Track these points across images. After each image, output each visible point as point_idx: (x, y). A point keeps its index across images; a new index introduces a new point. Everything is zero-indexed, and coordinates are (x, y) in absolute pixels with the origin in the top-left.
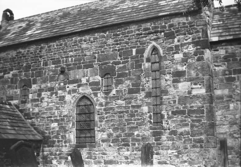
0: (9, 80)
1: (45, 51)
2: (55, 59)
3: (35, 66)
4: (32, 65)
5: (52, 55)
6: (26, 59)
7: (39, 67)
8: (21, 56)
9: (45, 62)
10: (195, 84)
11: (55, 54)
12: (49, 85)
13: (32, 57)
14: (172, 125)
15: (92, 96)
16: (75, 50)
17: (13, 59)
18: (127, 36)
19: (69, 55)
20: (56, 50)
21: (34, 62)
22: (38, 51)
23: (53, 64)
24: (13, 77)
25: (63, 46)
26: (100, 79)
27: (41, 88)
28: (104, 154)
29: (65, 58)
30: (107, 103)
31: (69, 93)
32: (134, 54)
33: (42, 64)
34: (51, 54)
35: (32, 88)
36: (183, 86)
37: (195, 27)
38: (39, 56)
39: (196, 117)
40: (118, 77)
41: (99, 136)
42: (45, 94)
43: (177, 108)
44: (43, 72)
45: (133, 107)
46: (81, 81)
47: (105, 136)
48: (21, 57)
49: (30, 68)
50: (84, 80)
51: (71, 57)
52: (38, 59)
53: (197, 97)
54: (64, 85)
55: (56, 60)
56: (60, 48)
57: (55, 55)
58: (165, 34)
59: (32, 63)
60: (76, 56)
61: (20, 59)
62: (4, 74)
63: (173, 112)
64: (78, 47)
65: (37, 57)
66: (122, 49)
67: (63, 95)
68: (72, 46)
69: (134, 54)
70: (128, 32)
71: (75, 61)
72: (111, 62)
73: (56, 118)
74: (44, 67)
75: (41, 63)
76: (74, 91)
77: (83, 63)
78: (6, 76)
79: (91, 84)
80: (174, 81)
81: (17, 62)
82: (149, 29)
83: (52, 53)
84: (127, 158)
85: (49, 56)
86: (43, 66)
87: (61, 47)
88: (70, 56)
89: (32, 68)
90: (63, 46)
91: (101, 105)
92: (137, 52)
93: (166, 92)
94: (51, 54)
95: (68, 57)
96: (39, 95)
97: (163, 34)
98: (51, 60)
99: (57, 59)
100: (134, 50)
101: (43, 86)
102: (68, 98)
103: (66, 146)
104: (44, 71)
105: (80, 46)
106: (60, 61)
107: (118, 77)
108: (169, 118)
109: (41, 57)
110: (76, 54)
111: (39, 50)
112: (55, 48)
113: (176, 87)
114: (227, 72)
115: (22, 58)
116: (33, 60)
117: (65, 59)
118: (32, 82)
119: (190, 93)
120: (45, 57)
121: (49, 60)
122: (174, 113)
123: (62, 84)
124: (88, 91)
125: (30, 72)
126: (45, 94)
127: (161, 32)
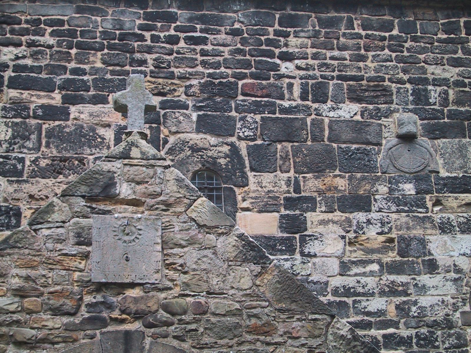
1: (309, 38)
2: (362, 78)
3: (259, 93)
4: (240, 83)
5: (347, 62)
6: (204, 53)
7: (282, 98)
8: (172, 32)
9: (311, 82)
11: (363, 58)
12: (342, 183)
16: (456, 63)
17: (122, 38)
19: (431, 77)
20: (362, 42)
21: (253, 76)
22: (271, 29)
23: (358, 100)
25: (395, 32)
27: (297, 190)
29: (411, 83)
33: (297, 91)
34: (336, 53)
35: (252, 186)
38: (277, 51)
42: (323, 223)
44: (304, 121)
49: (234, 97)
51: (437, 82)
52: (276, 67)
54: (417, 193)
55: (364, 82)
56: (383, 39)
57: (361, 64)
59: (243, 76)
60: (457, 84)
61: (168, 46)
62: (69, 100)
65: (272, 55)
67: (418, 232)
68: (440, 41)
71: (458, 102)
73: (391, 330)
74: (309, 103)
75: (290, 86)
81: (150, 58)
83: (346, 54)
85: (328, 61)
86: (304, 97)
87: (387, 34)
88: (434, 80)
89: (240, 97)
90: (395, 32)
94: (336, 53)
98: (339, 78)
99: (370, 80)
104: (309, 120)
106: (386, 92)
109: (287, 57)
110: (458, 75)
111: (277, 26)
112: (359, 36)
115: (182, 44)
116: (247, 65)
117: (408, 86)
118: (246, 158)
120: (310, 62)
121: (333, 78)
123: (409, 189)
125: (233, 114)
126: (323, 223)
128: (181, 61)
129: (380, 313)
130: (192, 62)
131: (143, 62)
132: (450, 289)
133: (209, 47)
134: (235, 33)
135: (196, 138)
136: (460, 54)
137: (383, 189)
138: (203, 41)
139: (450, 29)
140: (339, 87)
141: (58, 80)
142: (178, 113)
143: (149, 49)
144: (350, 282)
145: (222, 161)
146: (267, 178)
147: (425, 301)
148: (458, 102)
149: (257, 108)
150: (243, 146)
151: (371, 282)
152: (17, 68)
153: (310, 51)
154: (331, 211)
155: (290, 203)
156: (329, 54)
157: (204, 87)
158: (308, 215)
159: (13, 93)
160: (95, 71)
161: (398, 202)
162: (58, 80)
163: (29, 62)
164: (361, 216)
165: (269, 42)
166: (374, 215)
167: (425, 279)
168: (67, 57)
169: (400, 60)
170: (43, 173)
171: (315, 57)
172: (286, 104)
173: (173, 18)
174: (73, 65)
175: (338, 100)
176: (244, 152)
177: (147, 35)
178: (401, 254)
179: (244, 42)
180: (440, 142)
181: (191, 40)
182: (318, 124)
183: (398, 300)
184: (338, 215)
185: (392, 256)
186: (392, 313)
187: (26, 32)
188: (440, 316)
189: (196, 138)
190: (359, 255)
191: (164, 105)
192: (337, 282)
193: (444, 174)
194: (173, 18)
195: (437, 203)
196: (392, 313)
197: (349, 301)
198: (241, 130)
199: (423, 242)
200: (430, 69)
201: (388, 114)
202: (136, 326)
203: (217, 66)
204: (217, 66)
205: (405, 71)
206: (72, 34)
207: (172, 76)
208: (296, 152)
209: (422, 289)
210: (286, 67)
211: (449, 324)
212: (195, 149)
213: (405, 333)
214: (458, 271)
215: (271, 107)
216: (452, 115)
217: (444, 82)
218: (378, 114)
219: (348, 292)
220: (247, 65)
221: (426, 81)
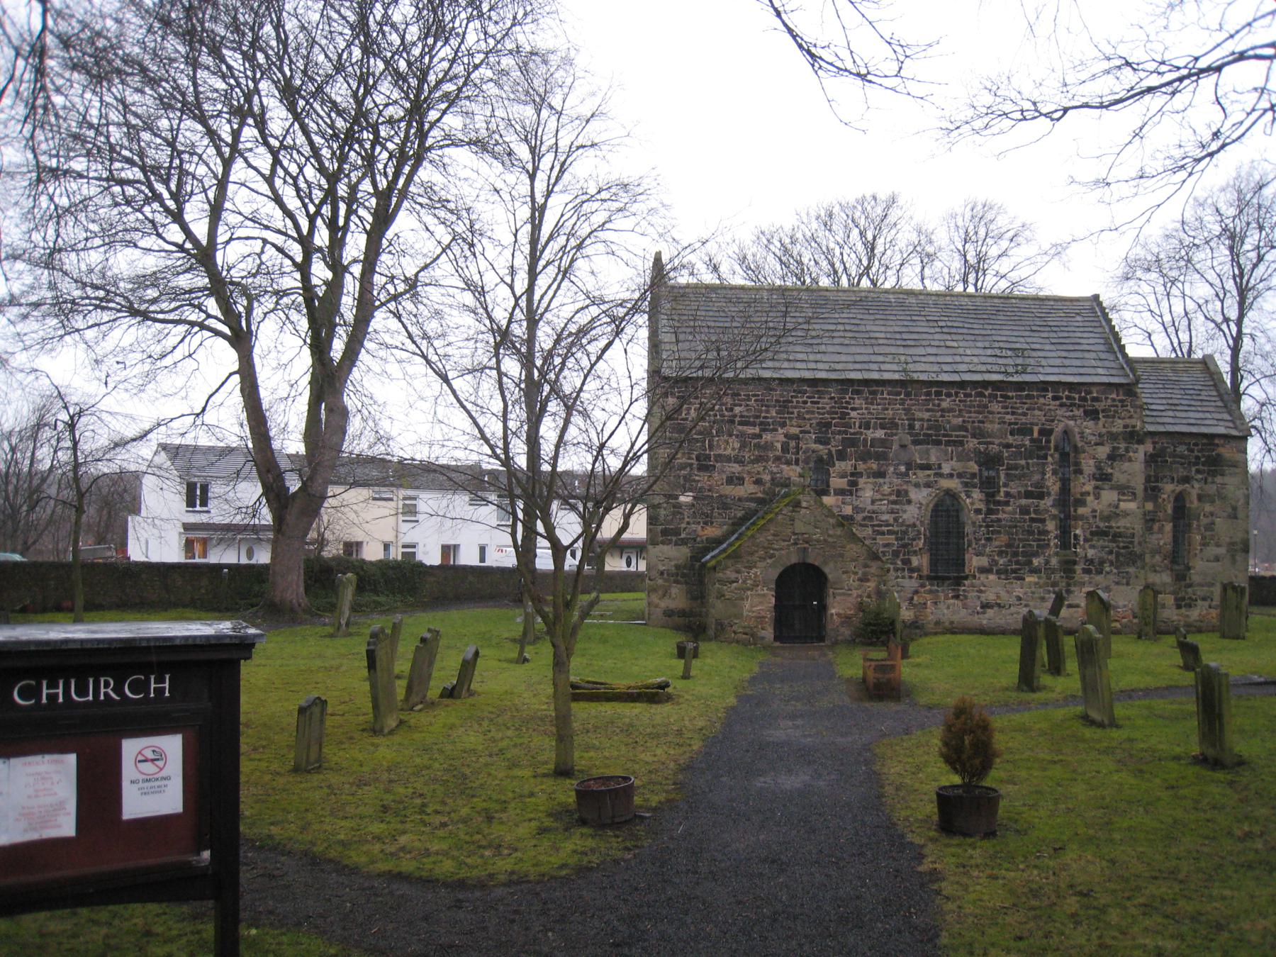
0: (779, 446)
10: (1124, 494)
11: (887, 409)
12: (875, 466)
13: (834, 407)
14: (1091, 553)
15: (963, 496)
16: (928, 410)
17: (784, 401)
18: (1025, 403)
21: (839, 418)
23: (883, 428)
24: (784, 440)
26: (976, 467)
27: (855, 468)
28: (981, 591)
30: (990, 512)
31: (917, 485)
32: (1036, 435)
36: (1109, 496)
37: (1129, 408)
39: (1123, 542)
40: (1008, 469)
41: (974, 561)
42: (866, 483)
43: (1097, 527)
45: (1032, 520)
46: (940, 467)
47: (984, 561)
48: (805, 402)
50: (946, 469)
52: (849, 414)
53: (1126, 514)
58: (1086, 413)
59: (834, 419)
60: (929, 420)
62: (764, 430)
63: (1092, 533)
64: (934, 405)
65: (847, 408)
66: (1016, 424)
67: (905, 487)
69: (1036, 435)
70: (1027, 395)
72: (997, 441)
76: (928, 485)
77: (944, 436)
78: (767, 437)
79: (960, 476)
80: (1096, 488)
81: (796, 411)
82: (1062, 398)
84: (1019, 599)
86: (860, 427)
91: (978, 511)
92: (1041, 432)
93: (1081, 502)
95: (914, 420)
96: (853, 484)
97: (1082, 410)
100: (1036, 429)
101: (861, 467)
102: (914, 495)
103: (911, 577)
105: (939, 405)
107: (1008, 469)
108: (1086, 540)
109: (853, 409)
113: (1097, 497)
114: (1153, 479)
116: (837, 413)
119: (1117, 507)
120: (864, 411)
122: (1092, 533)
123: (903, 468)
124: (954, 484)
126: (866, 483)
127: (1079, 406)
128: (808, 412)
129: (887, 521)
130: (813, 413)
131: (792, 413)
132: (917, 511)
133: (820, 406)
134: (832, 398)
135: (814, 446)
136: (931, 406)
137: (892, 469)
138: (818, 403)
139: (928, 394)
140: (876, 423)
141: (758, 421)
142: (807, 436)
143: (796, 407)
144: (875, 507)
145: (825, 457)
146: (843, 464)
147: (905, 516)
148: (927, 429)
149: (839, 433)
150: (833, 450)
151: (884, 508)
152: (741, 416)
153: (864, 406)
154: (869, 477)
155: (852, 474)
156: (872, 407)
157: (818, 424)
158: (860, 480)
159: (740, 428)
160: (772, 418)
161: (897, 474)
162: (758, 421)
163: (746, 414)
164: (881, 480)
165: (847, 402)
166: (887, 480)
167: (906, 507)
168: (761, 411)
169: (904, 409)
170: (752, 462)
171: (866, 409)
172: (852, 431)
173: (805, 392)
174: (763, 415)
175: (875, 428)
176: (834, 452)
177: (794, 400)
178: (897, 496)
179: (836, 403)
180: (918, 447)
181: (812, 402)
182: (865, 440)
183: (893, 515)
184: (871, 480)
185: (893, 497)
186: (891, 521)
187: (744, 400)
188: (911, 521)
189: (814, 446)
190: (879, 497)
191: (801, 432)
192: (870, 507)
193: (919, 461)
194: (805, 392)
195: (915, 474)
196: (891, 521)
197: (874, 516)
198: (833, 443)
199: (906, 492)
200: (917, 413)
201: (896, 434)
202: (806, 545)
203: (823, 414)
204: (823, 414)
205: (906, 415)
206: (762, 400)
207: (805, 418)
208: (856, 452)
209: (905, 511)
210: (853, 414)
211: (914, 525)
212: (813, 451)
213: (896, 529)
214: (921, 504)
215: (846, 432)
216: (925, 435)
217: (922, 420)
218: (892, 435)
219: (874, 512)
220: (837, 413)
221: (914, 420)
